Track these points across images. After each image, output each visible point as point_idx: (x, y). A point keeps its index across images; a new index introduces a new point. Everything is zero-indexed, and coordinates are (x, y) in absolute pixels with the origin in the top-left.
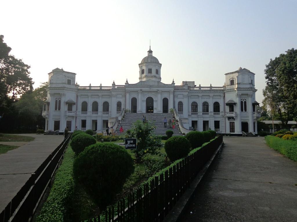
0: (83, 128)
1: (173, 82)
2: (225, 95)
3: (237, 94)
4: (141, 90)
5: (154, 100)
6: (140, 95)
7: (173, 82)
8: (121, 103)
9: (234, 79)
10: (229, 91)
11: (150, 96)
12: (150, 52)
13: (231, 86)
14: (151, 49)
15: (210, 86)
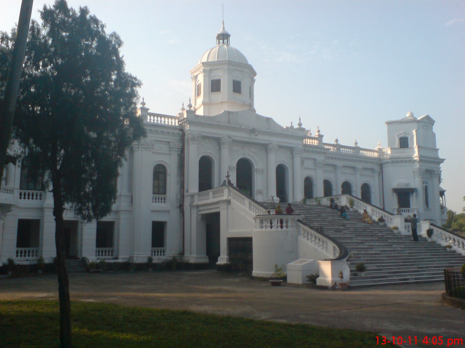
0: (23, 249)
1: (300, 124)
2: (384, 169)
3: (419, 169)
4: (229, 137)
5: (255, 168)
6: (225, 151)
7: (300, 124)
8: (164, 167)
9: (407, 136)
10: (397, 161)
11: (247, 156)
12: (224, 37)
13: (402, 150)
14: (226, 29)
15: (353, 145)
